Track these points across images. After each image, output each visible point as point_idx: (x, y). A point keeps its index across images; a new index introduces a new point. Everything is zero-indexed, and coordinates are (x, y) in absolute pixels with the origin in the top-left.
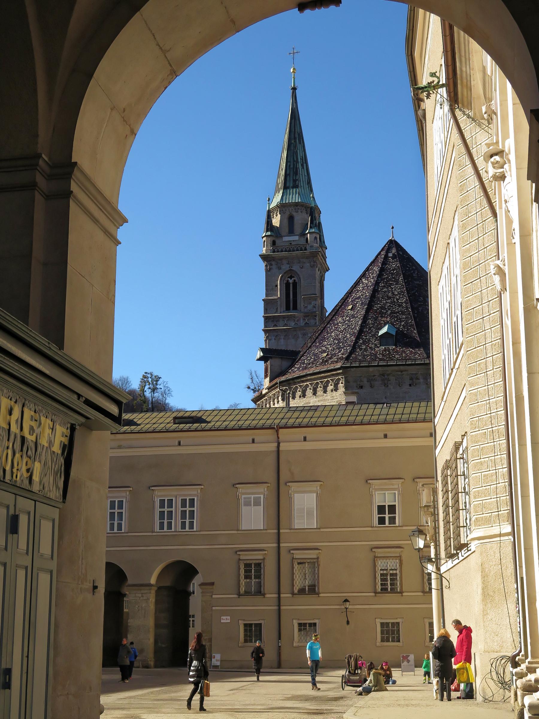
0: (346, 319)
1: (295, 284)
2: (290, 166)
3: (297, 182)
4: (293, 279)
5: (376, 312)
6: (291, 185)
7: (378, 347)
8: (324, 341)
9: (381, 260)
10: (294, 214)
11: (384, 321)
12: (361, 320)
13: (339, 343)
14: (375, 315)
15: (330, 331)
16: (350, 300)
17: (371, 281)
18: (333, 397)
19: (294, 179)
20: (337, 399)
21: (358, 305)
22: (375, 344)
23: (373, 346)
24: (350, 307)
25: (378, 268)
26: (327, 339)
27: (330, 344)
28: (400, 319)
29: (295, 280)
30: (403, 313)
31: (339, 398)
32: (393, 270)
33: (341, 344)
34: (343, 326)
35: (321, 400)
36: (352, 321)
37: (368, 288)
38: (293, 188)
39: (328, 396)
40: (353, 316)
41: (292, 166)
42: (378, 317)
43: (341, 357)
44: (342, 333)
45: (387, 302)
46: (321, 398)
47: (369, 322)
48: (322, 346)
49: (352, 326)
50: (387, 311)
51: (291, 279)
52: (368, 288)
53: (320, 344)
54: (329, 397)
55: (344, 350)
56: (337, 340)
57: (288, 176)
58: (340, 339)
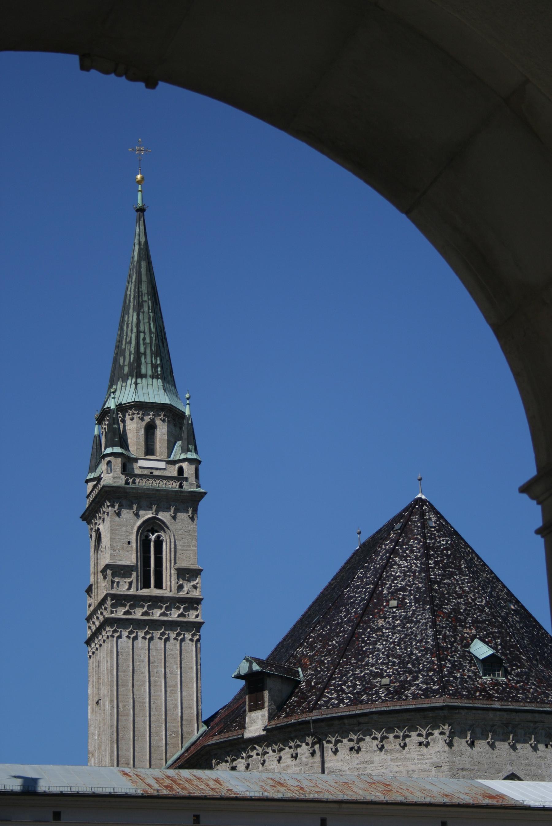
0: (394, 622)
1: (159, 543)
2: (144, 339)
3: (159, 369)
4: (156, 534)
5: (449, 617)
6: (149, 373)
7: (481, 678)
8: (365, 657)
9: (418, 530)
10: (158, 422)
11: (468, 634)
12: (431, 627)
13: (403, 663)
14: (451, 622)
15: (368, 639)
16: (385, 592)
17: (416, 564)
18: (423, 755)
19: (154, 362)
20: (431, 758)
21: (407, 601)
22: (472, 671)
23: (470, 674)
24: (394, 603)
25: (418, 543)
26: (372, 653)
27: (382, 664)
28: (492, 633)
29: (159, 537)
30: (491, 624)
31: (435, 759)
32: (447, 549)
33: (409, 665)
34: (393, 634)
35: (397, 758)
36: (411, 628)
37: (414, 575)
38: (152, 377)
39: (412, 753)
40: (408, 619)
41: (148, 340)
42: (456, 627)
43: (427, 688)
44: (398, 645)
45: (458, 603)
46: (397, 755)
47: (445, 633)
48: (367, 664)
49: (416, 636)
50: (466, 619)
51: (153, 534)
52: (414, 575)
53: (359, 660)
54: (414, 755)
55: (423, 675)
56: (393, 656)
57: (143, 357)
58: (400, 656)
